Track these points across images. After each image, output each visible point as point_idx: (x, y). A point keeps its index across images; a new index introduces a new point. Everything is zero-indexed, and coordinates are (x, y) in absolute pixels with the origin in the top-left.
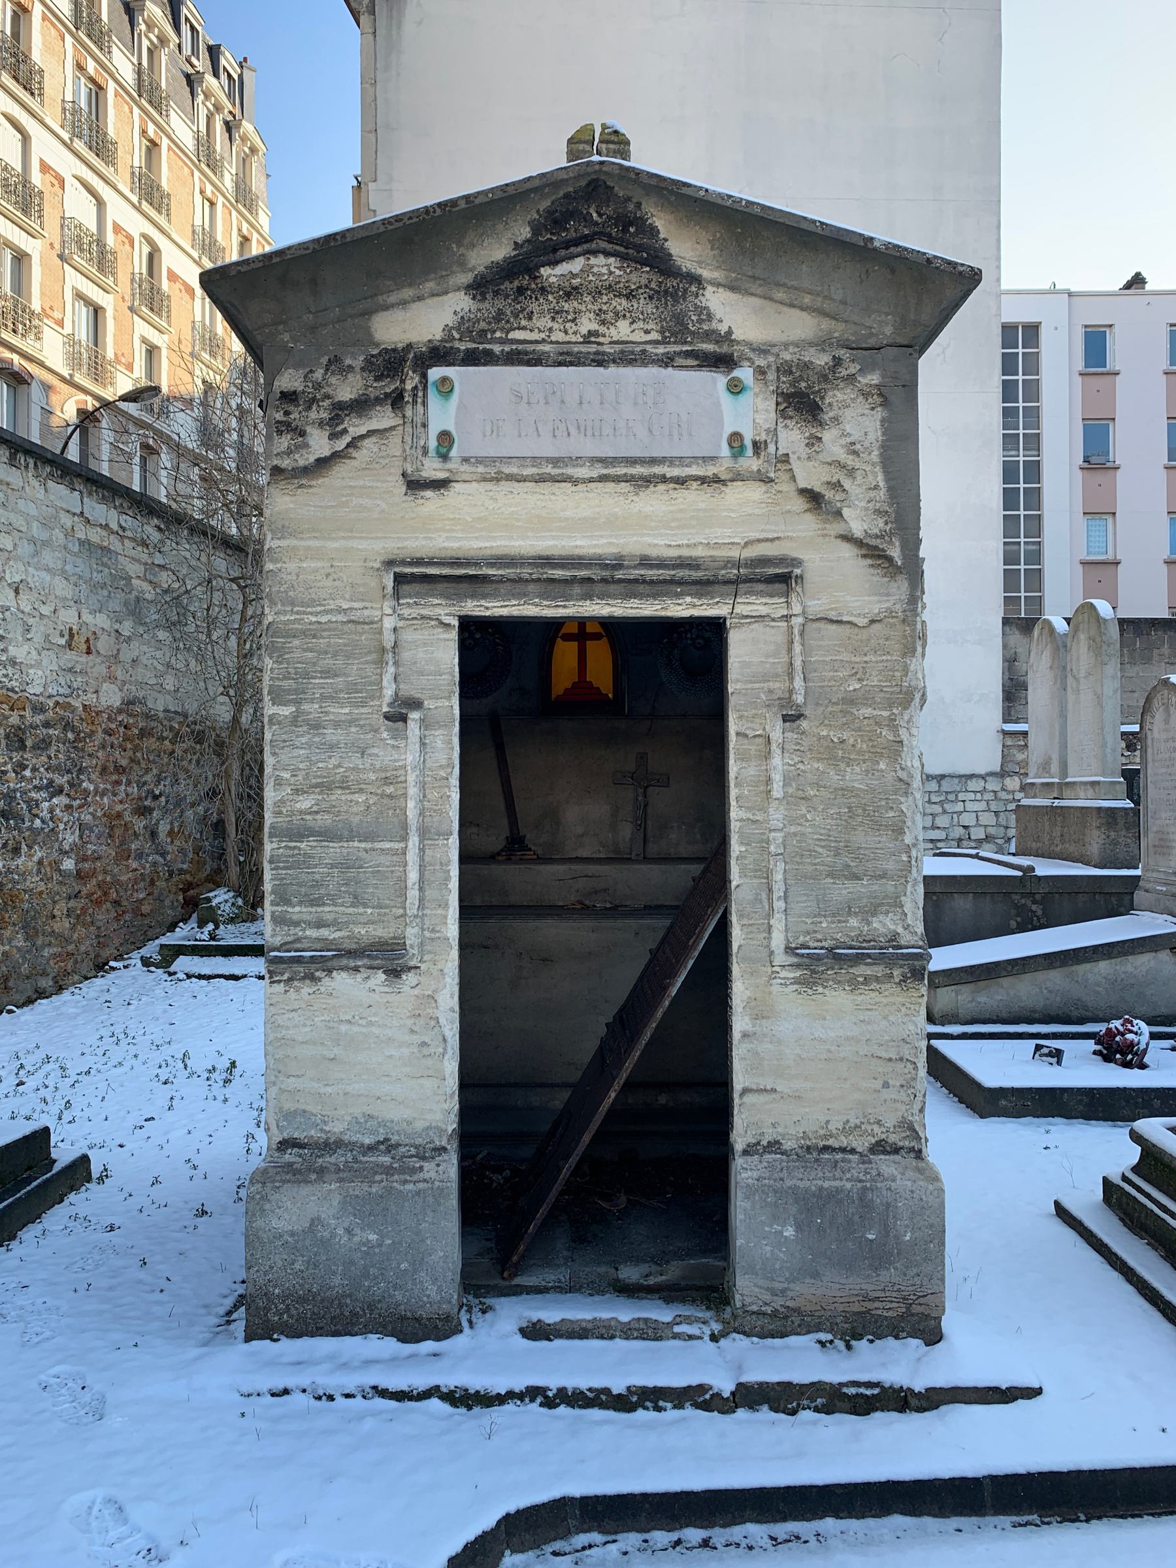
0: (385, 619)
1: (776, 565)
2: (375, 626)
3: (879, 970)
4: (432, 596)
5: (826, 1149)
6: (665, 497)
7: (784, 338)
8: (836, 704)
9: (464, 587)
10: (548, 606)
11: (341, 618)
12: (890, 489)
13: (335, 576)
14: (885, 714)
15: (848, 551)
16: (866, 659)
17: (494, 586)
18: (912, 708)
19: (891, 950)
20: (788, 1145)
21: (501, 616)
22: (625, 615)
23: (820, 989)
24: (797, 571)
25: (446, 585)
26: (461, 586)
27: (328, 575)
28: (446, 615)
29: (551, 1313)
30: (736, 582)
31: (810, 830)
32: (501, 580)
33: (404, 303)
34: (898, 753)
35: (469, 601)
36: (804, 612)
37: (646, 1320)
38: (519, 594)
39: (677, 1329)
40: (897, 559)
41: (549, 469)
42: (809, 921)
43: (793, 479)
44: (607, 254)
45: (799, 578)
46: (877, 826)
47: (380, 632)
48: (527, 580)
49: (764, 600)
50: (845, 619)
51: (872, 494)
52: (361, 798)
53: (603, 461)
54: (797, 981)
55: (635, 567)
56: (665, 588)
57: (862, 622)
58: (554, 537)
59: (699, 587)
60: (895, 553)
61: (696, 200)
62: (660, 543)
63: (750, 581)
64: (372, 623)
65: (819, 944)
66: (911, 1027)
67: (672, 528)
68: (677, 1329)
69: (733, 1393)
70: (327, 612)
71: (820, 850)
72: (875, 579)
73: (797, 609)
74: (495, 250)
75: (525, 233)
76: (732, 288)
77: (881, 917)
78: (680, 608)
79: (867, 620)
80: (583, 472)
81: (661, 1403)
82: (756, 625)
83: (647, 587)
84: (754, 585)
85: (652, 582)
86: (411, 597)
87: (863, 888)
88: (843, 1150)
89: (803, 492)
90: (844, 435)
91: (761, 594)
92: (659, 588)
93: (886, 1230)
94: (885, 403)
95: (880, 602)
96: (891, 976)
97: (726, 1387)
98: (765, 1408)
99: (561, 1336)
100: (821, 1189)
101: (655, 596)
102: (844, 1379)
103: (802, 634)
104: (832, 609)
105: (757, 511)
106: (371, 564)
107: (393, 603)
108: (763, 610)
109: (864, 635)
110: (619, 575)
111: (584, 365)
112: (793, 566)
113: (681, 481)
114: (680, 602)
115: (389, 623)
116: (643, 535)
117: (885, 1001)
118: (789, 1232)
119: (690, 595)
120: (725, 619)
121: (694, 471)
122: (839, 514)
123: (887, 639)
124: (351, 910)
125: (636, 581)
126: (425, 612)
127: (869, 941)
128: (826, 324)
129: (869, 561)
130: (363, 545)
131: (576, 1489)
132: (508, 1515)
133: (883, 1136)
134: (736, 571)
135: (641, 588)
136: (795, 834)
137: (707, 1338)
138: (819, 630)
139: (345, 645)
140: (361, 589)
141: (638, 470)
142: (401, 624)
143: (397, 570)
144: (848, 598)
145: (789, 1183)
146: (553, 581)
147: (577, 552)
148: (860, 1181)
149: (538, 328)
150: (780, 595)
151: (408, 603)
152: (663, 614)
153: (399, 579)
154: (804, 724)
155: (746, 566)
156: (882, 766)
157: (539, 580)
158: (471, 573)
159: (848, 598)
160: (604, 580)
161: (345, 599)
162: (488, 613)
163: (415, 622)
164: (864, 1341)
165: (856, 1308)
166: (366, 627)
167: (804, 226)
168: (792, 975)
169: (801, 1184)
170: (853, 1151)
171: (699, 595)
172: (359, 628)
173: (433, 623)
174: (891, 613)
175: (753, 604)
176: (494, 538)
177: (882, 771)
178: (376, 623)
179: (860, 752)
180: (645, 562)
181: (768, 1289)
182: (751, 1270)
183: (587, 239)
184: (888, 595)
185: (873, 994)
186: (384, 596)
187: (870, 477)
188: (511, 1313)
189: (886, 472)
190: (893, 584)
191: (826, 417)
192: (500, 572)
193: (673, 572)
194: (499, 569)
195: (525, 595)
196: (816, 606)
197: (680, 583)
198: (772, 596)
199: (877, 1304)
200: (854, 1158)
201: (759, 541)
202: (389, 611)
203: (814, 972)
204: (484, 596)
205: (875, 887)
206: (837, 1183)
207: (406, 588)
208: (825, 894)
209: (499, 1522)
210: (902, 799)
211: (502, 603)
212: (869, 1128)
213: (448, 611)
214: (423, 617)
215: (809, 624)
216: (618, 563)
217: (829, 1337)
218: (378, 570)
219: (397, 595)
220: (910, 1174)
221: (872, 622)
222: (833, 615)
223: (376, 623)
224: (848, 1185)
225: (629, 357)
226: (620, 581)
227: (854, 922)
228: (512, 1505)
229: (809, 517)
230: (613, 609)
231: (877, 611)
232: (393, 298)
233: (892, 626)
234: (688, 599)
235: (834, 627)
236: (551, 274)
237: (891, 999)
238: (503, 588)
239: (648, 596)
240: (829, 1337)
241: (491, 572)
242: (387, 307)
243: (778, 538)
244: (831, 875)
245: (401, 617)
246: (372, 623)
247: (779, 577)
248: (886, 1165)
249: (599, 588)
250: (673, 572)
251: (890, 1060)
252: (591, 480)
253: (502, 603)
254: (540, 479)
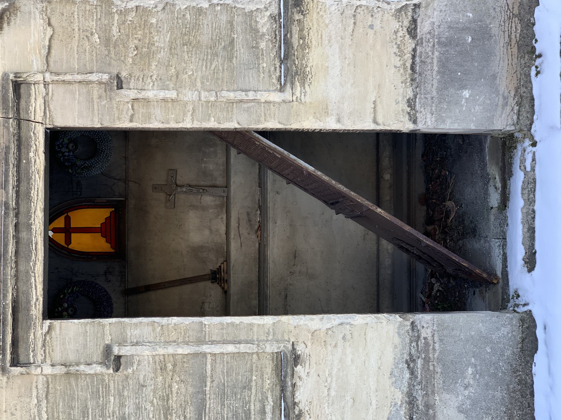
0: (45, 372)
1: (7, 91)
2: (50, 380)
3: (295, 29)
4: (28, 339)
5: (413, 68)
8: (109, 51)
9: (21, 316)
10: (36, 255)
11: (44, 404)
13: (13, 409)
14: (116, 17)
16: (77, 29)
17: (21, 295)
19: (282, 20)
20: (410, 94)
21: (44, 289)
22: (43, 200)
23: (308, 69)
24: (12, 76)
25: (19, 330)
26: (20, 319)
27: (12, 414)
28: (42, 329)
29: (518, 252)
30: (19, 120)
32: (16, 289)
34: (145, 9)
35: (32, 312)
36: (42, 72)
37: (523, 189)
38: (26, 277)
39: (529, 169)
42: (262, 75)
45: (17, 75)
46: (196, 26)
47: (54, 376)
48: (17, 271)
49: (33, 100)
50: (47, 43)
52: (175, 386)
54: (303, 85)
55: (7, 193)
56: (22, 171)
57: (49, 32)
59: (22, 147)
63: (18, 110)
64: (48, 382)
65: (278, 69)
66: (333, 8)
68: (529, 169)
71: (213, 66)
72: (18, 21)
73: (39, 77)
77: (259, 26)
78: (38, 160)
79: (48, 28)
82: (51, 106)
83: (22, 184)
84: (21, 107)
85: (18, 181)
86: (29, 355)
87: (239, 38)
88: (414, 57)
91: (28, 103)
92: (23, 176)
93: (465, 29)
95: (35, 19)
96: (299, 21)
99: (533, 245)
100: (439, 72)
101: (29, 179)
103: (58, 74)
104: (40, 53)
106: (4, 384)
107: (33, 367)
108: (40, 101)
109: (59, 30)
110: (12, 204)
112: (8, 79)
114: (33, 161)
115: (48, 370)
118: (466, 93)
119: (28, 154)
120: (47, 129)
123: (63, 14)
124: (253, 391)
125: (17, 193)
126: (40, 344)
127: (276, 35)
133: (405, 29)
134: (11, 120)
135: (23, 188)
136: (202, 83)
137: (534, 149)
138: (55, 62)
139: (64, 401)
140: (23, 390)
142: (49, 361)
143: (8, 365)
144: (32, 41)
145: (434, 93)
146: (17, 252)
148: (434, 46)
150: (29, 89)
151: (33, 356)
152: (42, 173)
153: (15, 362)
154: (124, 74)
155: (7, 113)
157: (16, 262)
158: (10, 311)
159: (32, 41)
160: (17, 215)
161: (30, 402)
162: (41, 299)
163: (47, 351)
164: (536, 45)
165: (515, 50)
166: (50, 386)
168: (299, 88)
170: (414, 50)
171: (29, 147)
172: (51, 391)
173: (48, 338)
174: (43, 11)
177: (157, 21)
178: (47, 379)
179: (144, 35)
181: (503, 108)
182: (491, 119)
184: (30, 13)
185: (311, 34)
186: (28, 374)
188: (519, 279)
190: (22, 9)
192: (10, 290)
193: (11, 166)
194: (7, 291)
195: (27, 272)
196: (37, 63)
197: (19, 160)
198: (30, 95)
199: (513, 37)
200: (418, 48)
202: (39, 370)
204: (28, 302)
205: (239, 29)
206: (435, 61)
207: (22, 359)
208: (244, 64)
210: (178, 8)
211: (34, 289)
212: (399, 39)
213: (39, 327)
214: (44, 345)
215: (50, 68)
217: (533, 68)
218: (8, 378)
219: (27, 364)
220: (429, 12)
221: (49, 24)
222: (44, 52)
223: (47, 379)
224: (436, 54)
226: (17, 203)
227: (263, 45)
230: (38, 208)
231: (42, 21)
233: (53, 10)
234: (31, 154)
235: (53, 51)
238: (22, 288)
239: (28, 183)
240: (533, 68)
244: (230, 60)
245: (44, 361)
246: (48, 382)
248: (423, 28)
249: (22, 219)
250: (11, 166)
251: (355, 23)
253: (34, 289)
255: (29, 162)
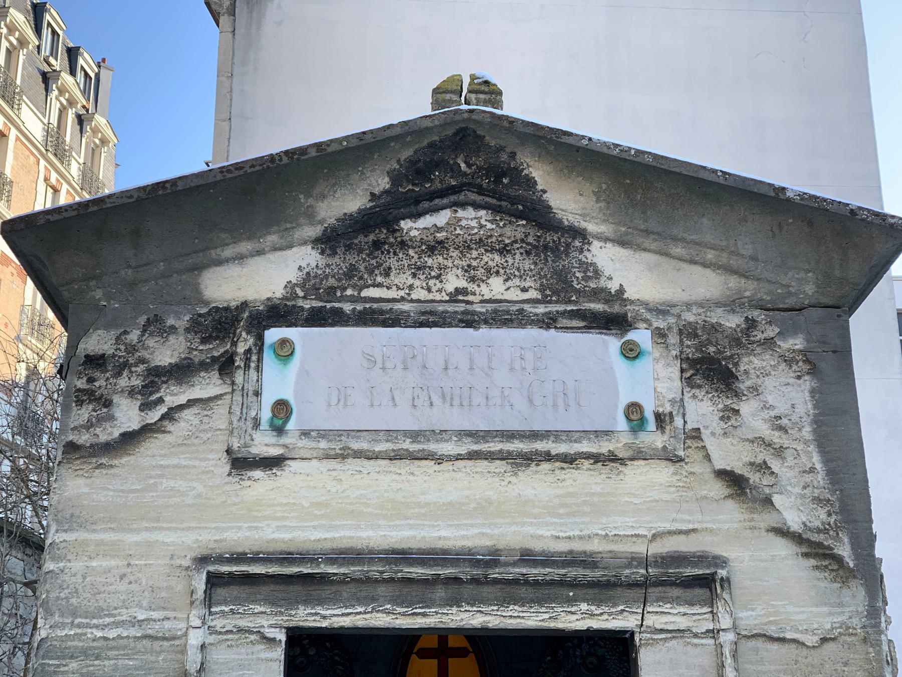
0: (192, 633)
1: (695, 565)
2: (177, 642)
4: (255, 602)
6: (551, 478)
7: (685, 297)
9: (296, 589)
10: (404, 614)
11: (135, 632)
13: (132, 578)
15: (783, 548)
17: (334, 588)
21: (342, 628)
22: (502, 626)
24: (722, 573)
25: (272, 587)
26: (291, 588)
27: (122, 577)
28: (271, 626)
30: (644, 584)
32: (344, 581)
35: (301, 608)
36: (735, 627)
38: (366, 597)
40: (847, 559)
41: (407, 445)
43: (708, 457)
44: (477, 206)
45: (726, 582)
47: (183, 651)
48: (376, 581)
49: (682, 609)
50: (789, 636)
51: (808, 478)
53: (473, 435)
55: (514, 564)
56: (553, 590)
58: (411, 527)
59: (596, 591)
60: (844, 550)
61: (578, 149)
62: (547, 533)
63: (663, 583)
64: (174, 638)
67: (560, 516)
70: (117, 624)
72: (822, 584)
73: (725, 622)
74: (348, 201)
75: (383, 183)
76: (622, 243)
78: (574, 617)
79: (816, 639)
80: (448, 448)
82: (674, 642)
83: (530, 590)
84: (668, 589)
85: (536, 583)
86: (226, 604)
89: (722, 474)
90: (766, 407)
91: (677, 601)
92: (546, 591)
94: (814, 371)
95: (831, 614)
101: (540, 602)
103: (735, 655)
104: (770, 623)
106: (178, 562)
107: (203, 611)
108: (683, 623)
109: (814, 657)
110: (495, 573)
111: (450, 325)
112: (717, 566)
113: (569, 460)
114: (573, 609)
115: (195, 638)
116: (524, 524)
119: (585, 600)
120: (632, 633)
122: (768, 502)
123: (846, 664)
125: (515, 582)
126: (243, 623)
128: (734, 282)
129: (813, 562)
130: (170, 538)
134: (643, 571)
135: (522, 591)
138: (757, 650)
139: (136, 669)
140: (163, 594)
142: (211, 639)
143: (211, 568)
144: (790, 609)
146: (409, 581)
147: (440, 544)
149: (396, 286)
150: (703, 603)
151: (222, 612)
152: (552, 625)
153: (214, 580)
155: (656, 564)
157: (392, 580)
158: (306, 571)
159: (790, 609)
160: (475, 581)
161: (141, 607)
162: (325, 624)
163: (230, 636)
166: (165, 643)
167: (703, 175)
171: (598, 602)
172: (157, 645)
173: (253, 637)
174: (847, 629)
175: (667, 615)
176: (334, 528)
178: (179, 638)
180: (527, 557)
184: (841, 605)
186: (192, 603)
187: (804, 459)
190: (845, 591)
192: (343, 570)
193: (563, 571)
194: (341, 565)
195: (373, 599)
196: (751, 618)
197: (573, 584)
198: (691, 604)
201: (671, 533)
202: (197, 622)
204: (321, 602)
207: (221, 592)
211: (344, 611)
213: (272, 622)
214: (241, 630)
215: (743, 641)
218: (187, 568)
219: (209, 601)
221: (824, 640)
222: (772, 631)
223: (179, 638)
225: (503, 317)
226: (496, 581)
229: (730, 504)
230: (487, 618)
231: (828, 626)
232: (228, 252)
233: (851, 645)
234: (584, 606)
235: (775, 646)
238: (346, 591)
239: (532, 601)
241: (331, 570)
242: (219, 262)
243: (694, 530)
245: (212, 631)
246: (174, 638)
247: (698, 579)
249: (469, 590)
250: (563, 571)
252: (459, 457)
253: (344, 611)
254: (396, 456)
255: (571, 601)
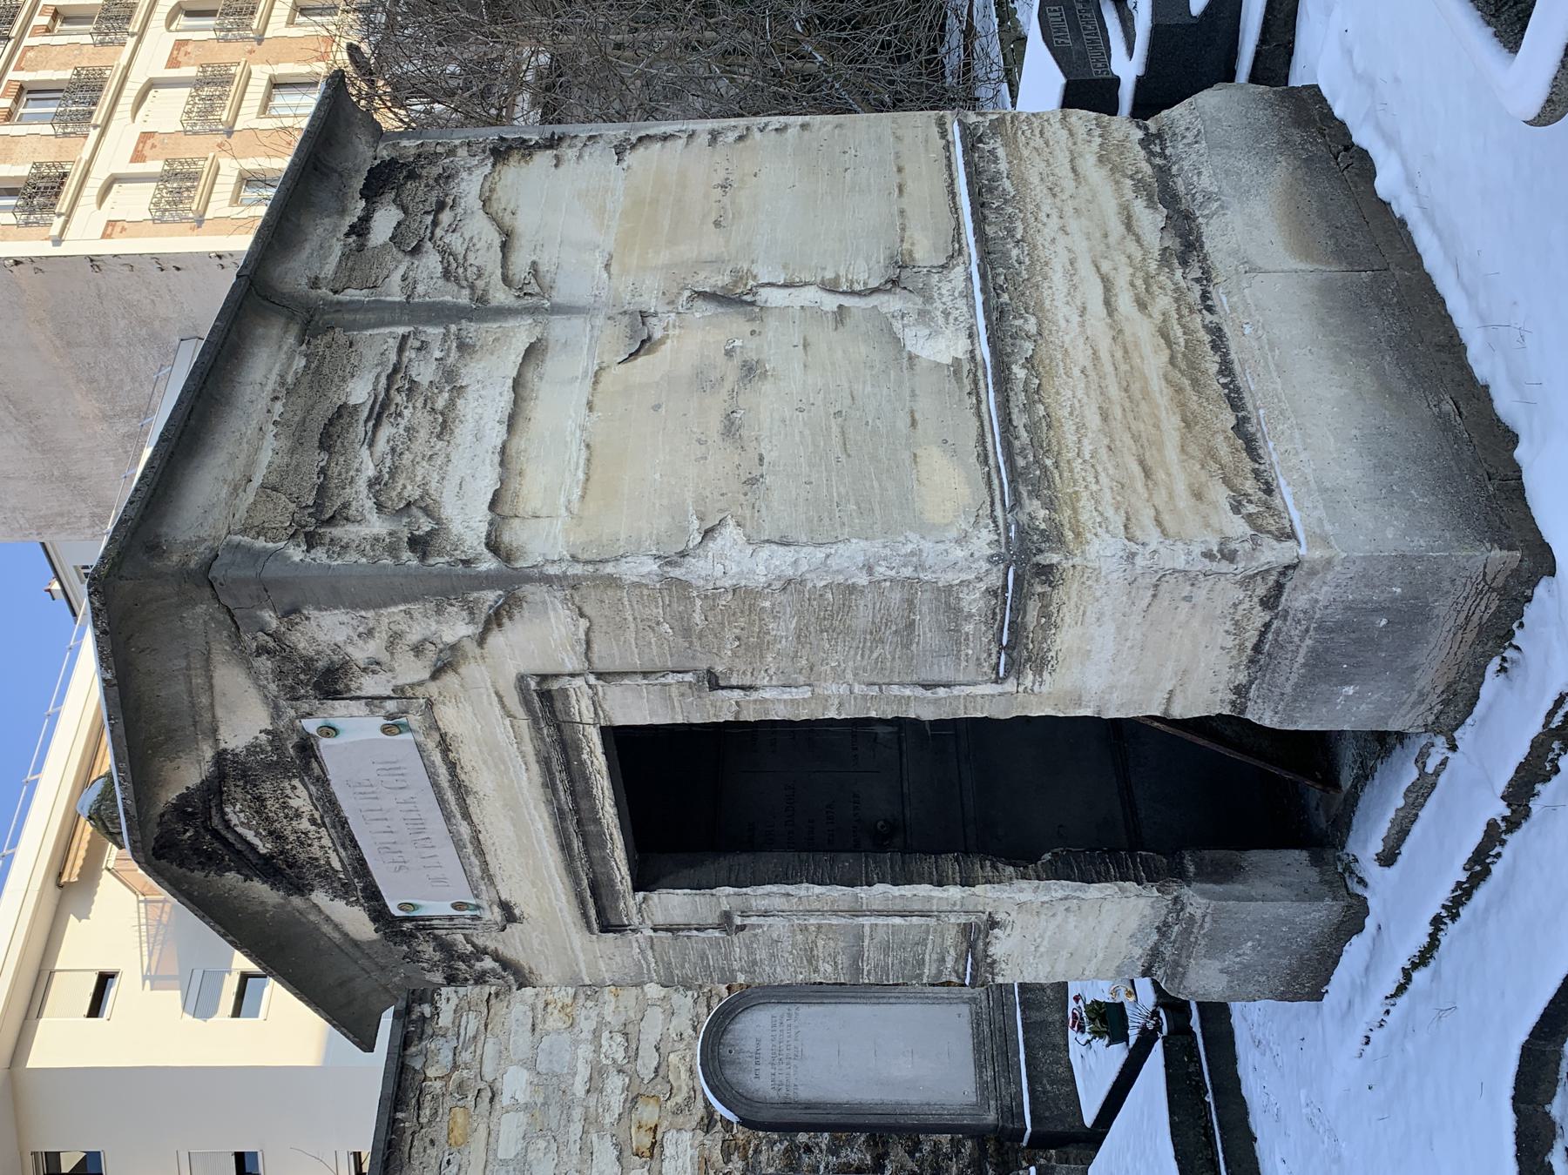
3: (1033, 608)
5: (1257, 648)
6: (474, 774)
7: (253, 691)
8: (691, 643)
11: (650, 953)
12: (405, 600)
14: (698, 602)
15: (496, 639)
16: (630, 618)
18: (688, 577)
19: (1009, 595)
20: (1242, 678)
23: (1052, 654)
31: (851, 664)
33: (337, 927)
34: (748, 591)
37: (1408, 790)
39: (1430, 769)
41: (470, 849)
42: (964, 664)
43: (421, 683)
44: (223, 814)
46: (846, 608)
49: (574, 702)
51: (416, 615)
52: (821, 943)
53: (448, 817)
54: (1039, 672)
57: (584, 623)
58: (539, 842)
60: (490, 597)
61: (137, 801)
62: (527, 781)
65: (994, 656)
66: (1115, 575)
67: (507, 769)
68: (1430, 769)
69: (1509, 805)
70: (645, 959)
71: (875, 655)
72: (526, 614)
74: (262, 891)
75: (231, 876)
76: (215, 731)
77: (964, 604)
80: (464, 829)
81: (1493, 853)
87: (925, 621)
88: (1263, 634)
89: (435, 676)
90: (350, 641)
93: (1379, 610)
94: (296, 610)
95: (555, 609)
96: (1042, 595)
97: (1500, 809)
98: (1538, 787)
99: (1399, 847)
100: (1304, 665)
102: (1541, 720)
105: (469, 709)
111: (350, 832)
113: (452, 766)
116: (521, 788)
117: (1074, 599)
118: (1349, 690)
121: (437, 757)
122: (454, 648)
124: (930, 946)
127: (994, 614)
128: (218, 658)
129: (505, 620)
130: (577, 944)
131: (1521, 1034)
132: (1514, 1098)
133: (1256, 600)
136: (855, 675)
137: (1450, 754)
141: (450, 796)
144: (556, 636)
145: (1288, 689)
147: (550, 827)
148: (1307, 630)
149: (325, 850)
154: (719, 669)
156: (767, 604)
164: (1517, 632)
165: (1470, 636)
167: (121, 730)
168: (1031, 677)
169: (1294, 678)
170: (1267, 625)
171: (579, 750)
175: (581, 709)
176: (550, 877)
177: (773, 605)
179: (752, 623)
180: (549, 784)
181: (1412, 708)
182: (1385, 720)
183: (216, 834)
185: (1064, 609)
187: (396, 618)
188: (1366, 842)
189: (386, 605)
191: (335, 658)
199: (1475, 618)
200: (1276, 624)
201: (503, 706)
203: (1029, 659)
204: (611, 881)
205: (925, 609)
206: (1303, 651)
208: (932, 651)
209: (1516, 1110)
210: (810, 585)
212: (1240, 612)
216: (559, 816)
217: (1497, 660)
220: (1313, 584)
221: (582, 615)
222: (581, 649)
224: (1309, 642)
225: (328, 803)
227: (969, 628)
228: (1507, 1091)
229: (463, 670)
232: (336, 935)
235: (595, 647)
236: (264, 847)
237: (1074, 594)
240: (1497, 660)
241: (585, 883)
242: (346, 935)
243: (497, 693)
244: (907, 646)
247: (543, 699)
248: (1296, 599)
251: (1154, 596)
252: (471, 823)
254: (480, 852)
255: (582, 763)
